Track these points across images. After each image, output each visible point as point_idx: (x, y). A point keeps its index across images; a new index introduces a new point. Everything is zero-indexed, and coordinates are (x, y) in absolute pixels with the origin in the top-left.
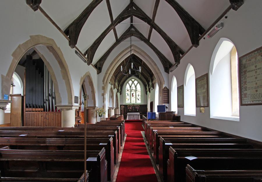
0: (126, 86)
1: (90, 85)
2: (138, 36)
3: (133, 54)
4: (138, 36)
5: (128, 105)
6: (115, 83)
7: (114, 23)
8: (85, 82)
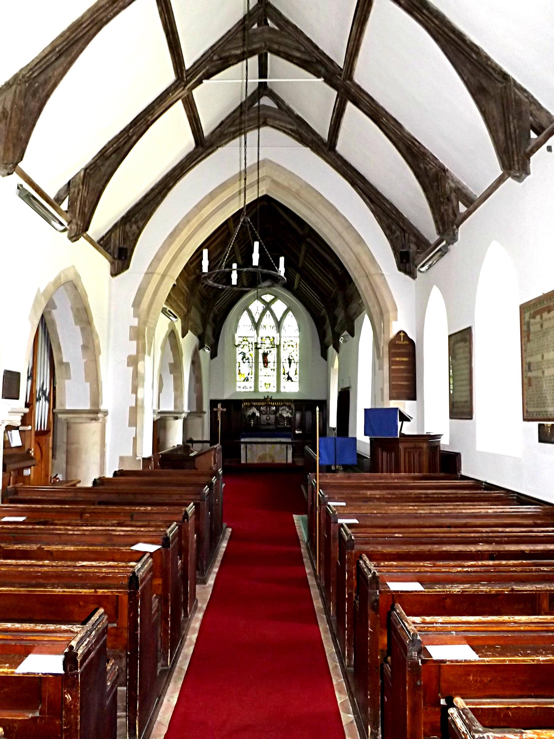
0: (238, 321)
1: (76, 323)
2: (289, 126)
3: (266, 198)
4: (289, 126)
5: (246, 401)
6: (189, 311)
7: (186, 79)
8: (55, 308)
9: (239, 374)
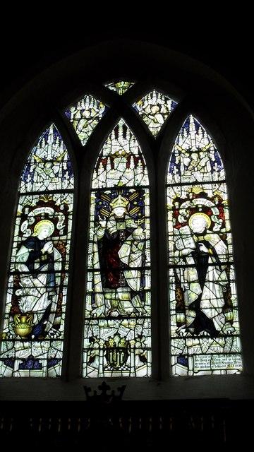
9: (12, 314)
